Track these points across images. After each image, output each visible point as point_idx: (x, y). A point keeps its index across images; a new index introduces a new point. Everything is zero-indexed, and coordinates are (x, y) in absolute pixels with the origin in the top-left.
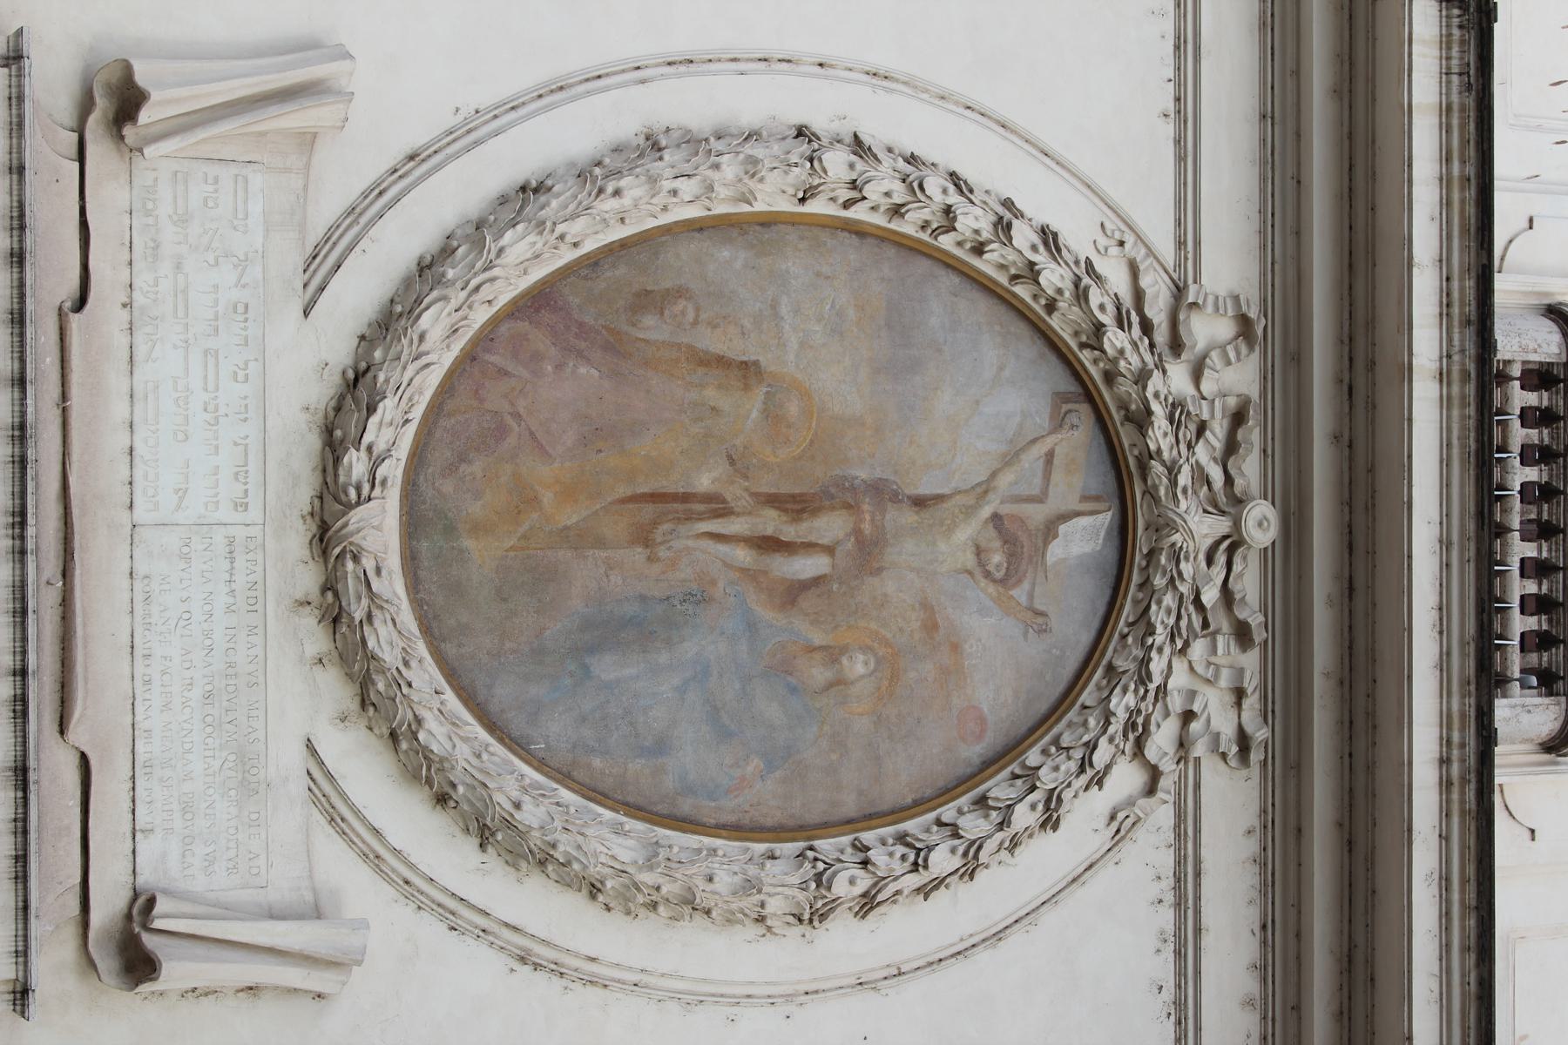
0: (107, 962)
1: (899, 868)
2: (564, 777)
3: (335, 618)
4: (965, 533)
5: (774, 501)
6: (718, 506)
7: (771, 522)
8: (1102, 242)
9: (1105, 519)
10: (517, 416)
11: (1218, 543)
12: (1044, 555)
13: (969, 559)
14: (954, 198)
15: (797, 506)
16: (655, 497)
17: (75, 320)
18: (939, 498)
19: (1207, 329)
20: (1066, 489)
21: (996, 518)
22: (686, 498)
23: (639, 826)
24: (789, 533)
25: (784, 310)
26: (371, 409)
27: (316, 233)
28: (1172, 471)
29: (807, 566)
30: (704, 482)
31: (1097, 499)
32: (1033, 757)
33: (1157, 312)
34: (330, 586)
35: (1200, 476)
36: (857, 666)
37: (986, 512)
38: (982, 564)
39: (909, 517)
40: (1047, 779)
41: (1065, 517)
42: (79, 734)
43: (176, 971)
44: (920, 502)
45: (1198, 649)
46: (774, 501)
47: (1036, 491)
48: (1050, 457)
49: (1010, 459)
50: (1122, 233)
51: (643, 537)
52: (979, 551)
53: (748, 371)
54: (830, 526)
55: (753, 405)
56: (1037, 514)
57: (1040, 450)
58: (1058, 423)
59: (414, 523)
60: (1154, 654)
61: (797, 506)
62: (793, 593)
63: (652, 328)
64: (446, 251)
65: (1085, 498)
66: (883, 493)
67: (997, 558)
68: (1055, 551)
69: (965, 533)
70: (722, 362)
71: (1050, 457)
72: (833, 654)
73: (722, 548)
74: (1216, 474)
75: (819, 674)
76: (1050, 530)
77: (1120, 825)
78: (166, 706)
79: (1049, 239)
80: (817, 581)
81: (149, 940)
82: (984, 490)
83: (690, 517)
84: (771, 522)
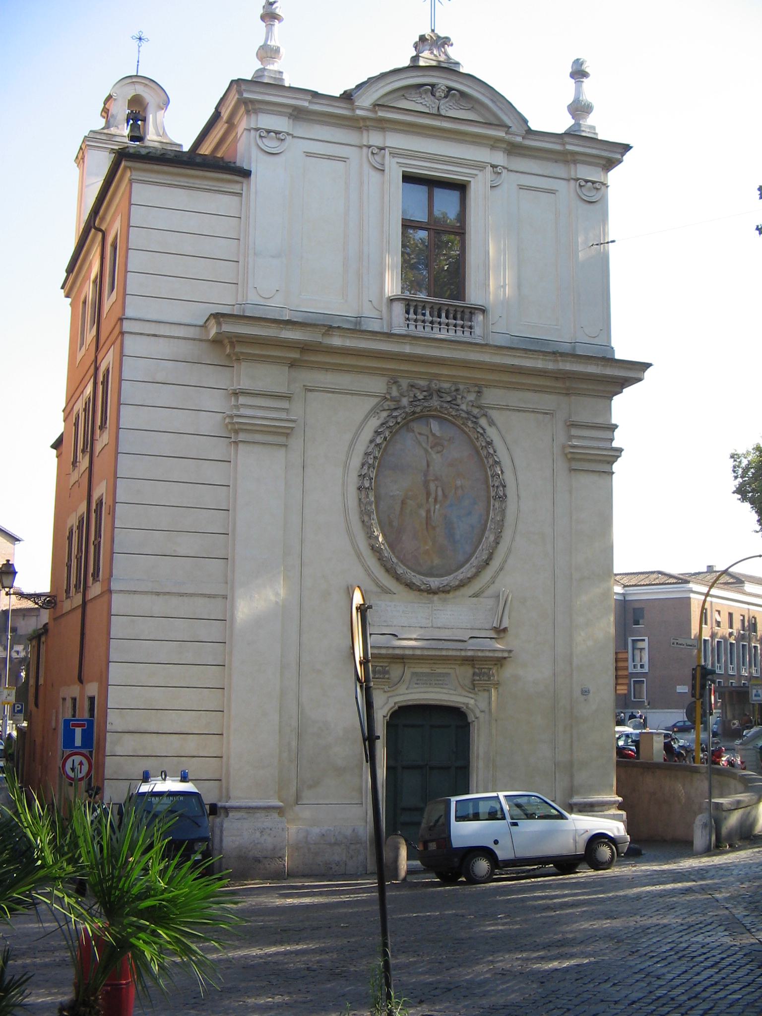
0: (502, 635)
1: (499, 480)
2: (477, 547)
3: (448, 592)
4: (434, 456)
5: (427, 499)
6: (428, 511)
7: (431, 500)
8: (377, 417)
9: (431, 420)
10: (412, 552)
11: (438, 395)
12: (439, 437)
13: (439, 455)
14: (372, 457)
15: (428, 494)
16: (427, 524)
17: (399, 637)
18: (427, 461)
19: (395, 393)
20: (424, 430)
21: (431, 448)
22: (427, 518)
23: (487, 532)
24: (433, 495)
25: (392, 494)
26: (414, 584)
27: (379, 590)
28: (426, 407)
29: (440, 493)
30: (423, 513)
31: (428, 423)
32: (478, 444)
33: (392, 405)
34: (443, 592)
35: (425, 399)
36: (459, 483)
37: (430, 450)
38: (440, 452)
39: (431, 468)
40: (484, 444)
41: (431, 431)
42: (466, 638)
43: (505, 624)
44: (428, 466)
45: (459, 401)
46: (427, 499)
47: (425, 437)
48: (420, 434)
49: (419, 443)
50: (374, 412)
51: (434, 528)
52: (438, 452)
53: (403, 503)
54: (432, 486)
55: (410, 502)
56: (431, 438)
57: (418, 436)
58: (413, 431)
59: (431, 575)
60: (462, 415)
61: (428, 494)
62: (445, 496)
63: (395, 524)
64: (385, 566)
65: (427, 426)
66: (426, 474)
67: (439, 448)
68: (438, 434)
69: (434, 456)
70: (402, 508)
71: (420, 434)
72: (456, 488)
73: (436, 510)
74: (425, 393)
75: (460, 492)
76: (434, 435)
77: (492, 423)
78: (462, 623)
79: (377, 433)
80: (443, 490)
81: (502, 628)
82: (426, 451)
83: (430, 518)
84: (431, 500)
